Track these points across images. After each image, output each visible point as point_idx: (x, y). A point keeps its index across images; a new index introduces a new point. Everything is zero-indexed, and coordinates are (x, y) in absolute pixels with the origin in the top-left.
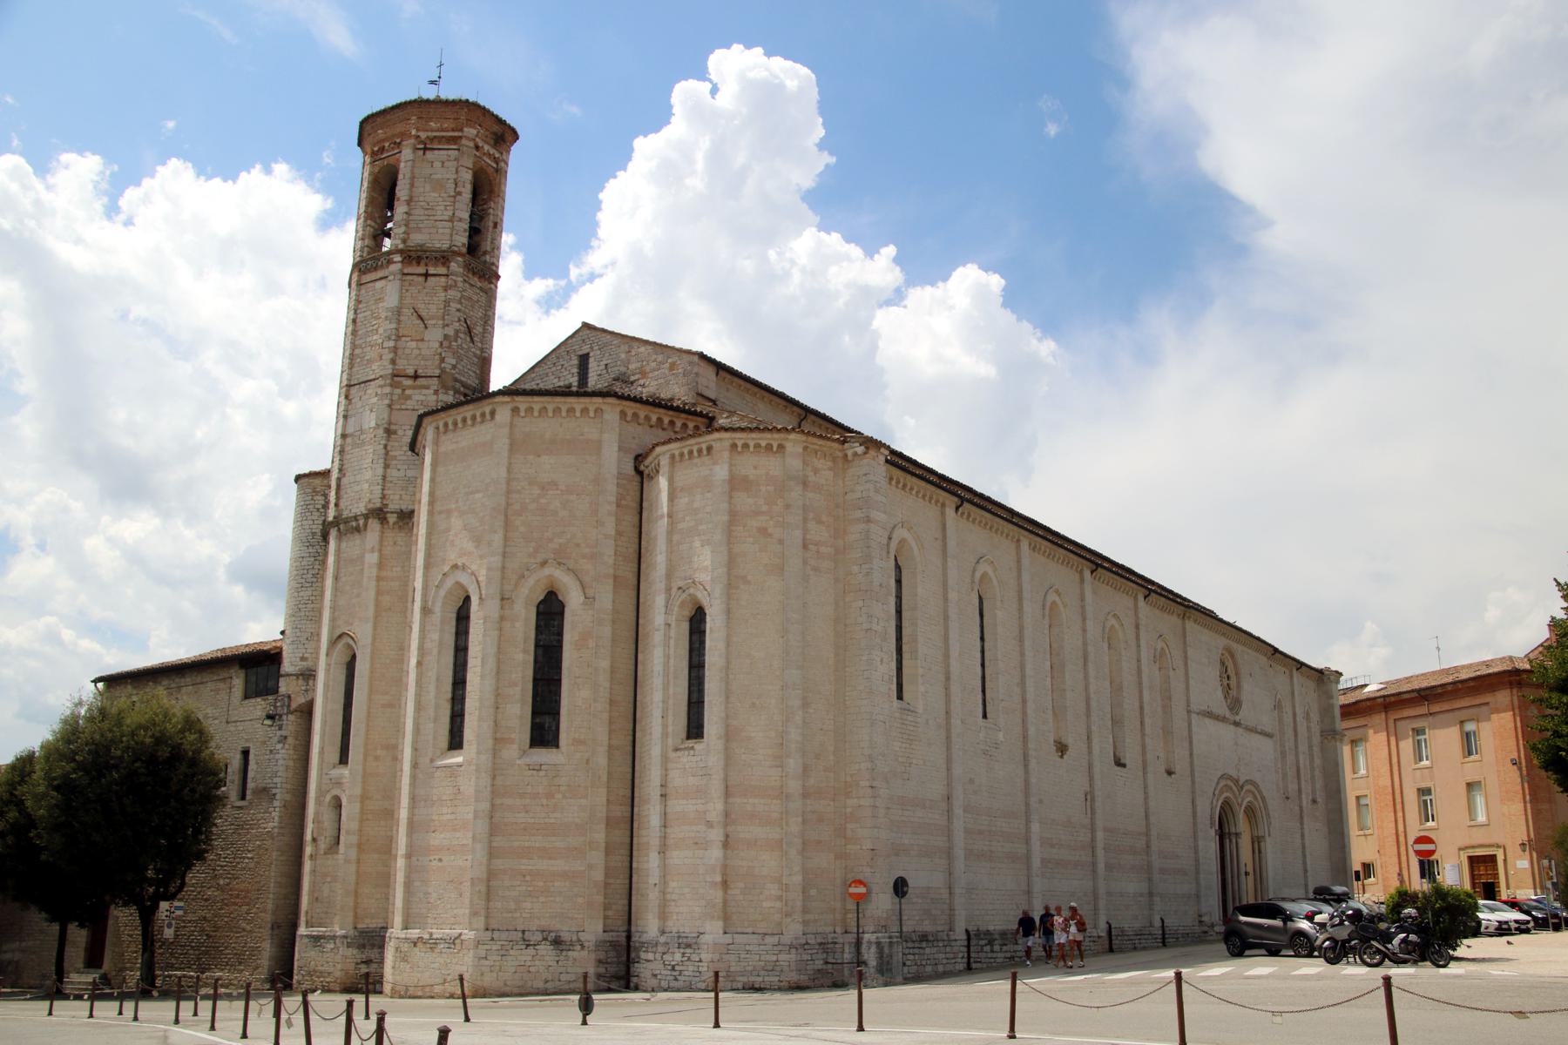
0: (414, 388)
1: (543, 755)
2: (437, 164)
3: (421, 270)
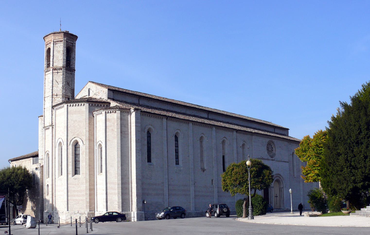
0: (56, 98)
2: (58, 47)
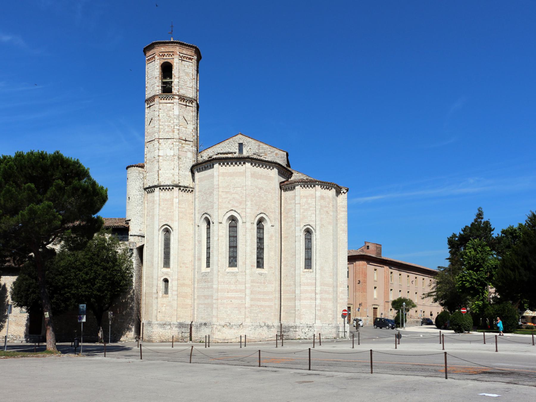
0: (185, 144)
1: (260, 270)
3: (185, 103)
